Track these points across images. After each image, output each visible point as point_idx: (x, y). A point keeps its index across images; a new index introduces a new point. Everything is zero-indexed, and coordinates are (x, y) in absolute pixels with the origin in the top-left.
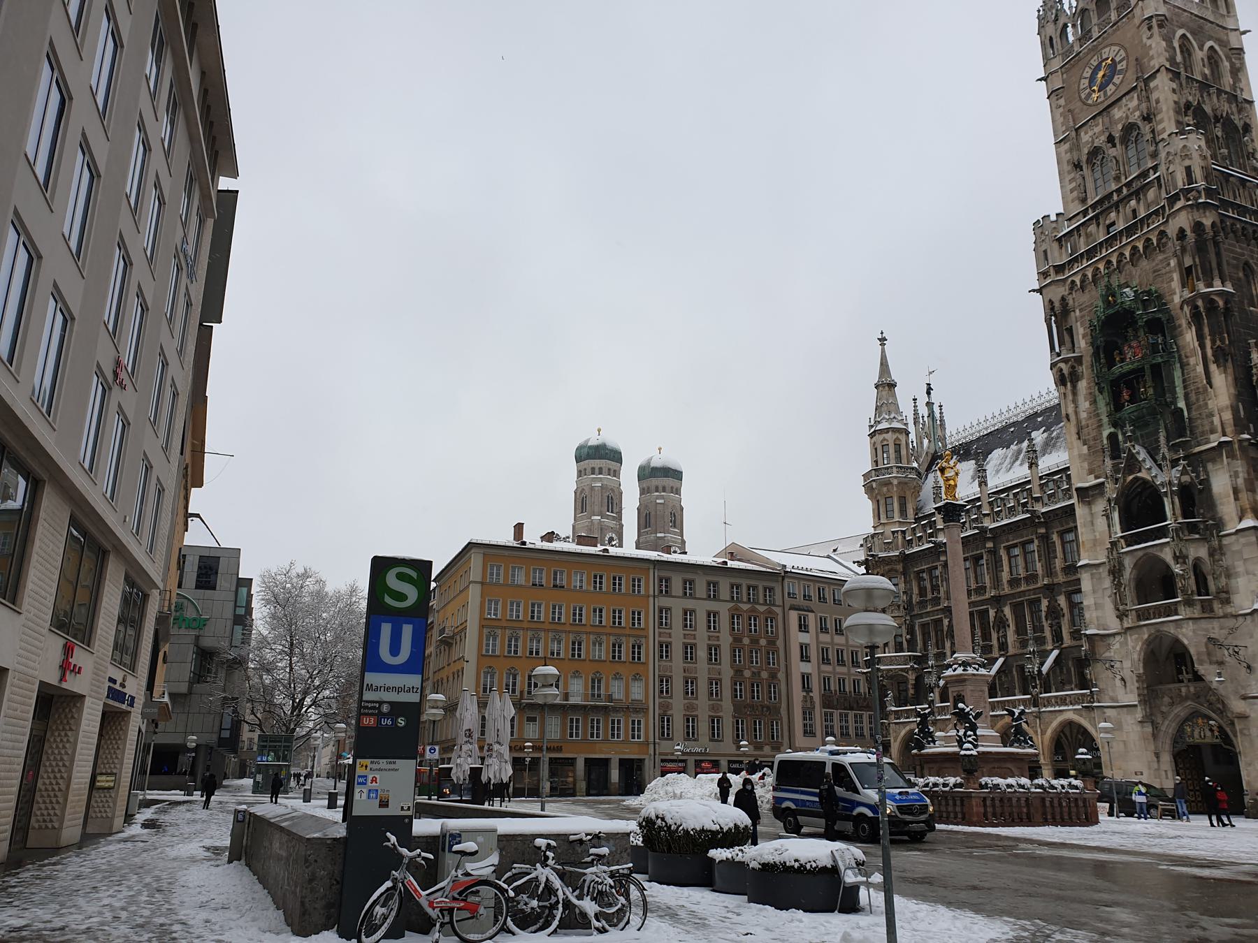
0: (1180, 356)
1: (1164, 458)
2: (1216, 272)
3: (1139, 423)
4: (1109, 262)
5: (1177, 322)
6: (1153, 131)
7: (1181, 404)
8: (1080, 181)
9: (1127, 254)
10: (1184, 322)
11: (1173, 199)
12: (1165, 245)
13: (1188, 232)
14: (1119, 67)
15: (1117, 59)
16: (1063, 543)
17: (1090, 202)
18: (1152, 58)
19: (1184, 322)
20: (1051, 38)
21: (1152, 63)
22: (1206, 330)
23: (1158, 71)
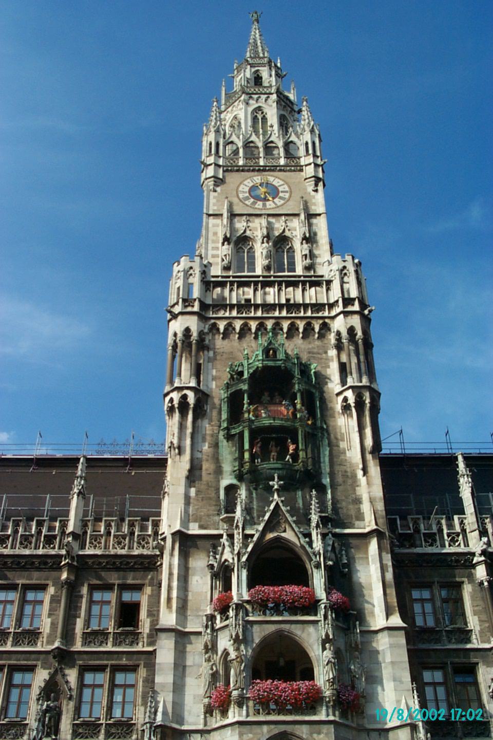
5: (330, 405)
6: (310, 251)
7: (326, 481)
10: (338, 405)
13: (359, 333)
14: (281, 195)
15: (281, 189)
16: (91, 602)
19: (338, 407)
20: (217, 144)
23: (320, 215)
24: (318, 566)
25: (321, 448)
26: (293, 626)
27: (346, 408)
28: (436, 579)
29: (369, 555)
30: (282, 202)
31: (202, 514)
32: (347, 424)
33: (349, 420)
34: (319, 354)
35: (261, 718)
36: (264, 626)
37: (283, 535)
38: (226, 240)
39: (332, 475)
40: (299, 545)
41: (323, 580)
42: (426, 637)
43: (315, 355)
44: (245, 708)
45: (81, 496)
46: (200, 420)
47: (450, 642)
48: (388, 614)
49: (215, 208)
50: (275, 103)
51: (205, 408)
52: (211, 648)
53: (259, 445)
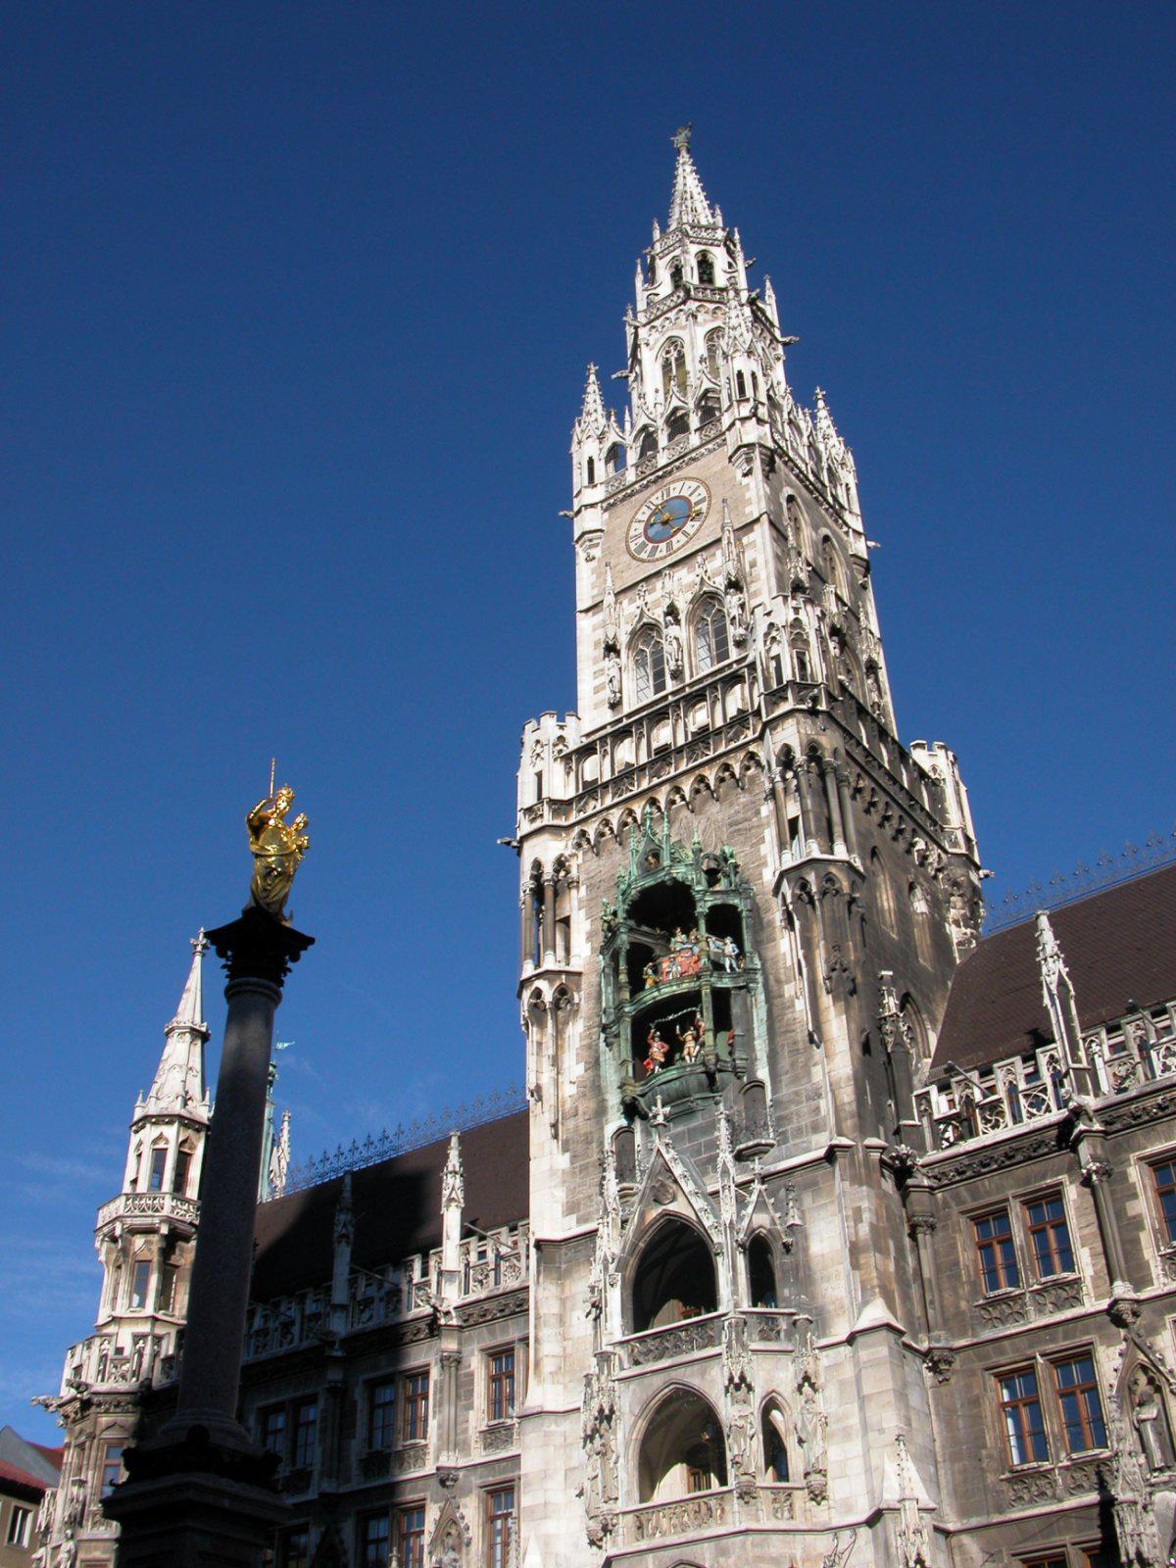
1: (725, 1172)
2: (837, 830)
3: (682, 1106)
4: (653, 802)
5: (766, 917)
6: (742, 606)
7: (763, 1073)
8: (614, 672)
11: (775, 696)
12: (752, 779)
13: (799, 757)
15: (693, 499)
17: (626, 709)
18: (749, 502)
19: (777, 916)
20: (591, 462)
21: (748, 510)
22: (818, 930)
25: (754, 1010)
26: (689, 1369)
28: (1010, 1193)
30: (697, 524)
34: (746, 820)
35: (643, 1545)
36: (647, 1380)
37: (672, 1207)
38: (611, 649)
40: (694, 1218)
42: (996, 1314)
43: (740, 826)
45: (453, 1204)
47: (1040, 1311)
49: (595, 592)
51: (576, 1000)
53: (657, 1039)
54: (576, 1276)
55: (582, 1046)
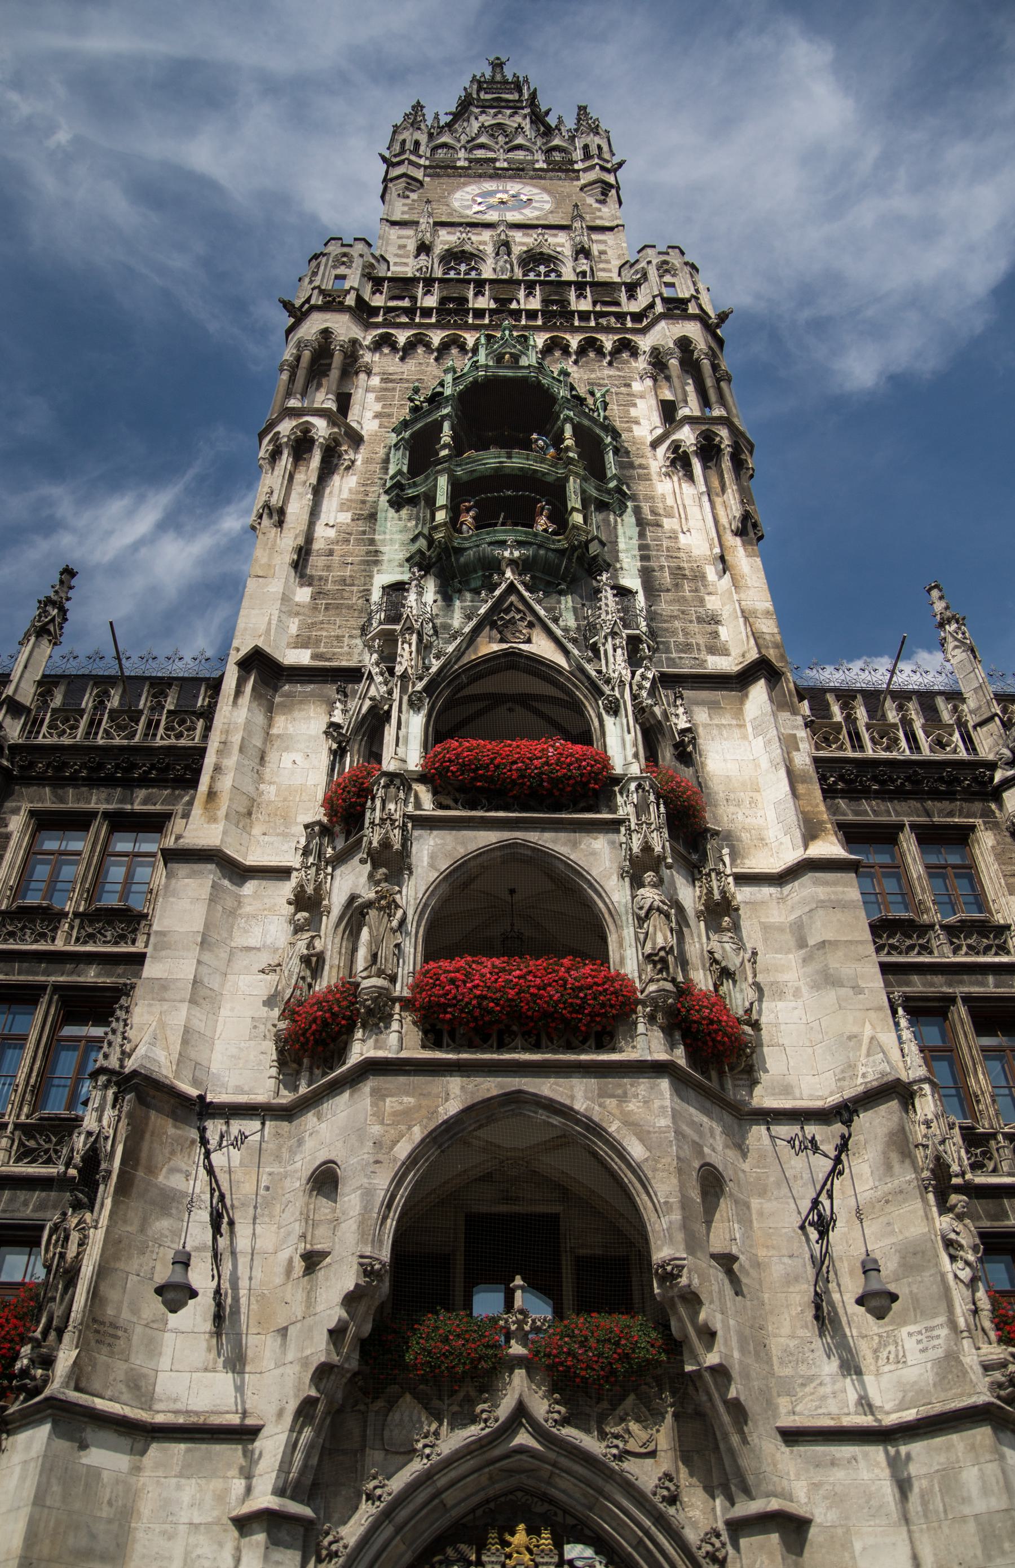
0: (637, 511)
5: (638, 461)
7: (631, 581)
9: (540, 340)
19: (657, 461)
23: (611, 229)
24: (614, 709)
25: (619, 527)
27: (680, 461)
28: (906, 820)
29: (747, 719)
31: (325, 634)
32: (677, 491)
33: (684, 485)
37: (524, 647)
39: (647, 575)
40: (566, 665)
41: (629, 738)
44: (395, 1026)
46: (336, 478)
48: (811, 833)
50: (528, 119)
52: (308, 904)
54: (296, 714)
55: (351, 501)
